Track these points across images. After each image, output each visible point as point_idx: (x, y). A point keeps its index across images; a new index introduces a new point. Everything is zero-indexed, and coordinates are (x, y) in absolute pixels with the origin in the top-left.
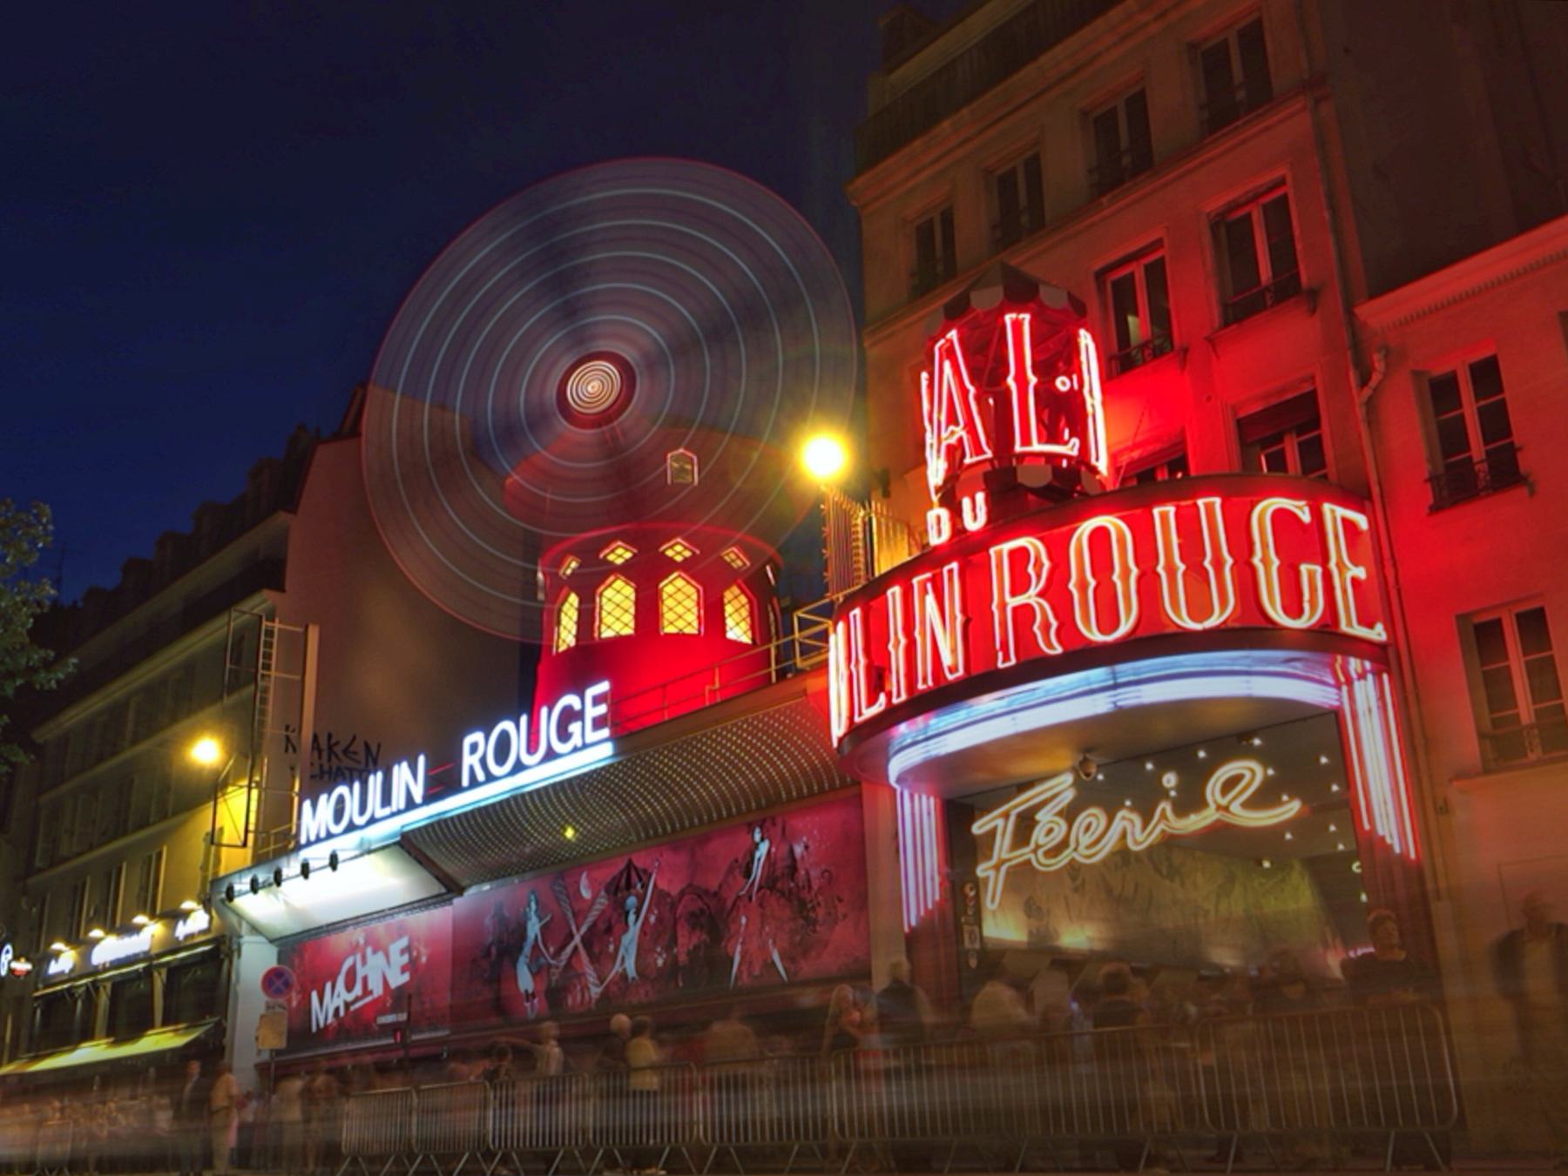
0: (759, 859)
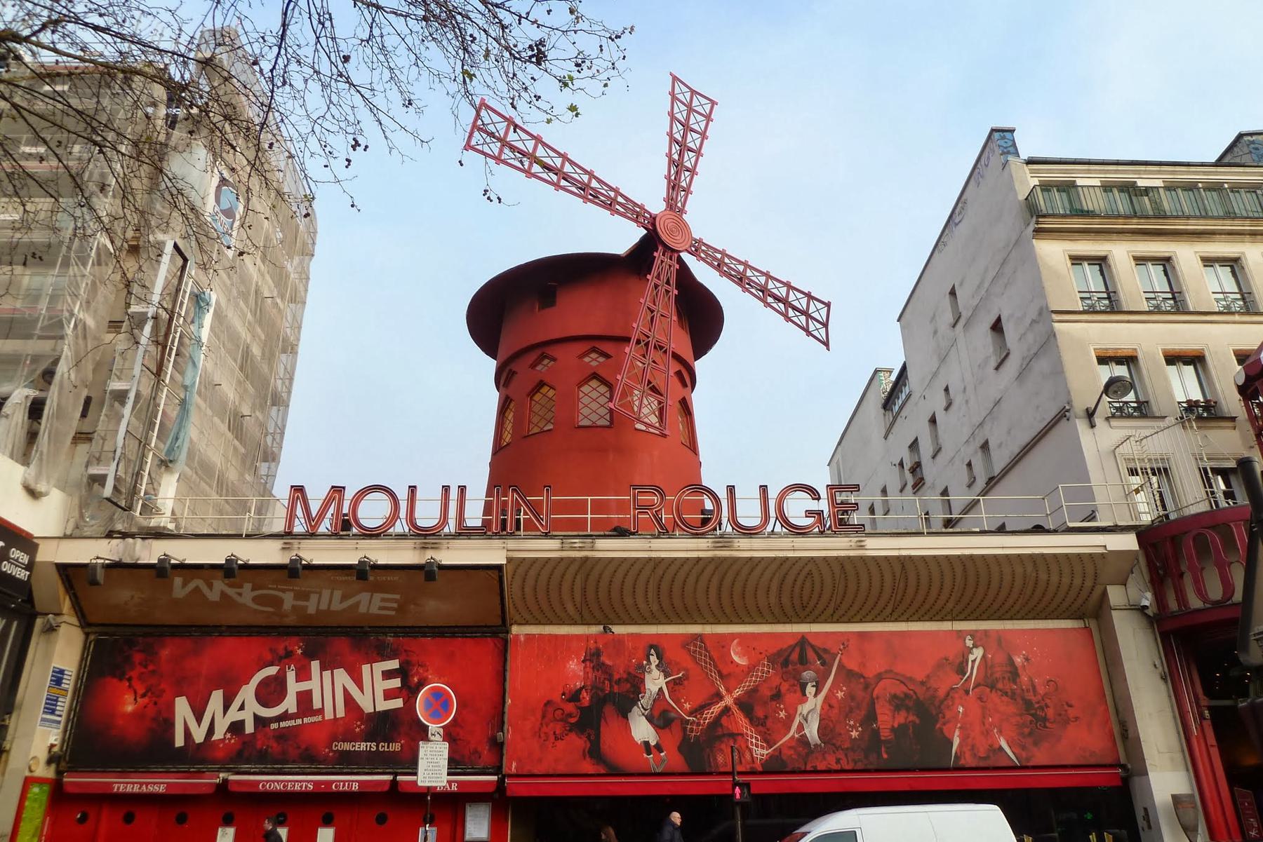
0: (974, 661)
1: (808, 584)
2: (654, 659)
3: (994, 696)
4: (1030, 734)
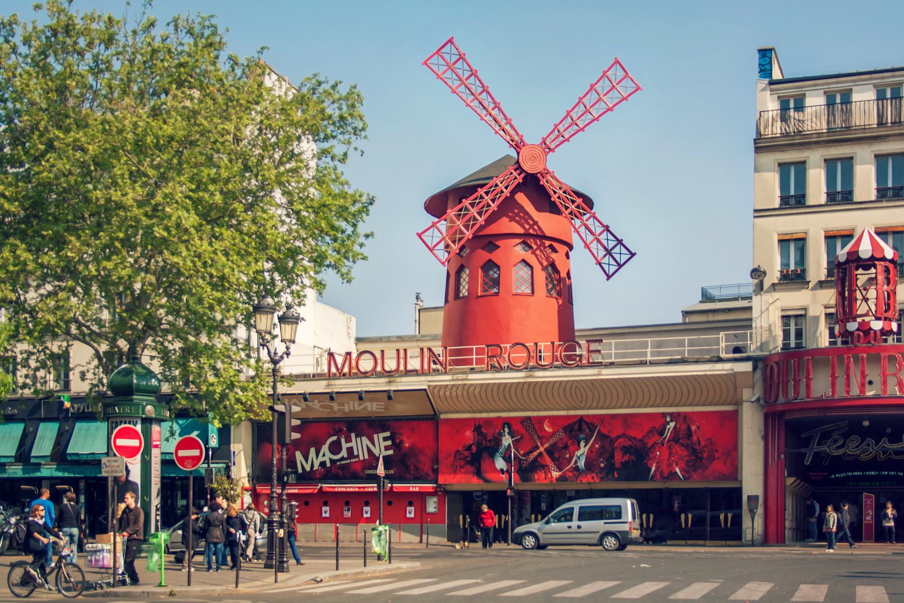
0: (669, 429)
1: (578, 392)
2: (507, 430)
3: (677, 447)
4: (693, 465)
